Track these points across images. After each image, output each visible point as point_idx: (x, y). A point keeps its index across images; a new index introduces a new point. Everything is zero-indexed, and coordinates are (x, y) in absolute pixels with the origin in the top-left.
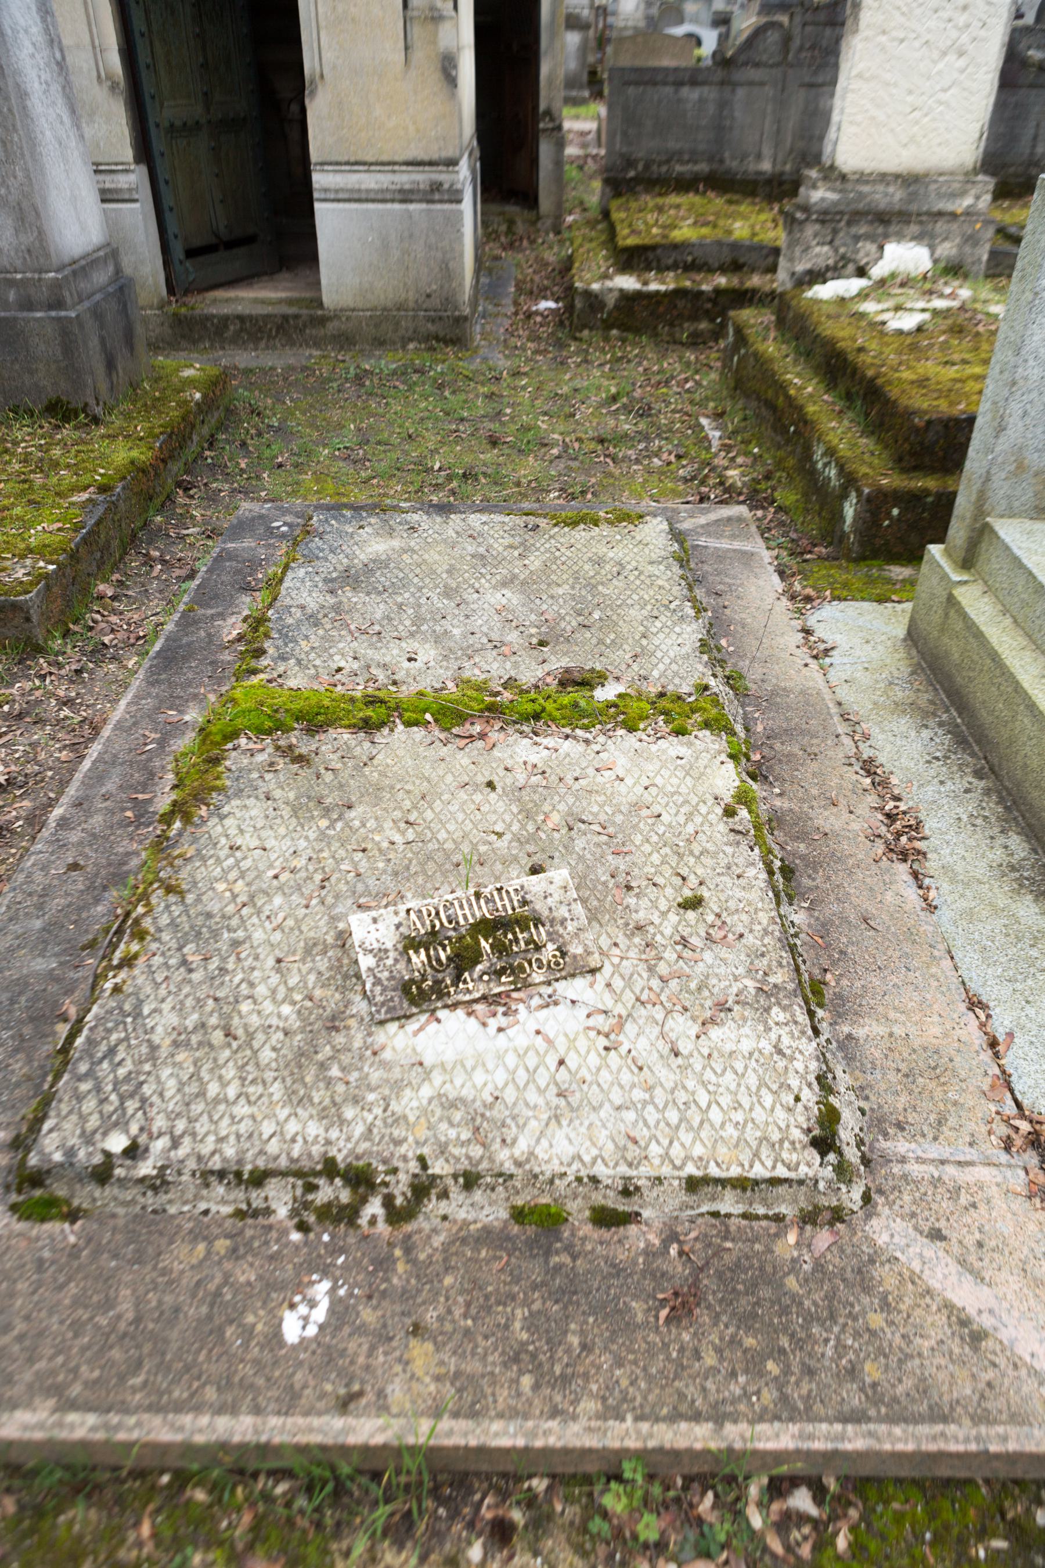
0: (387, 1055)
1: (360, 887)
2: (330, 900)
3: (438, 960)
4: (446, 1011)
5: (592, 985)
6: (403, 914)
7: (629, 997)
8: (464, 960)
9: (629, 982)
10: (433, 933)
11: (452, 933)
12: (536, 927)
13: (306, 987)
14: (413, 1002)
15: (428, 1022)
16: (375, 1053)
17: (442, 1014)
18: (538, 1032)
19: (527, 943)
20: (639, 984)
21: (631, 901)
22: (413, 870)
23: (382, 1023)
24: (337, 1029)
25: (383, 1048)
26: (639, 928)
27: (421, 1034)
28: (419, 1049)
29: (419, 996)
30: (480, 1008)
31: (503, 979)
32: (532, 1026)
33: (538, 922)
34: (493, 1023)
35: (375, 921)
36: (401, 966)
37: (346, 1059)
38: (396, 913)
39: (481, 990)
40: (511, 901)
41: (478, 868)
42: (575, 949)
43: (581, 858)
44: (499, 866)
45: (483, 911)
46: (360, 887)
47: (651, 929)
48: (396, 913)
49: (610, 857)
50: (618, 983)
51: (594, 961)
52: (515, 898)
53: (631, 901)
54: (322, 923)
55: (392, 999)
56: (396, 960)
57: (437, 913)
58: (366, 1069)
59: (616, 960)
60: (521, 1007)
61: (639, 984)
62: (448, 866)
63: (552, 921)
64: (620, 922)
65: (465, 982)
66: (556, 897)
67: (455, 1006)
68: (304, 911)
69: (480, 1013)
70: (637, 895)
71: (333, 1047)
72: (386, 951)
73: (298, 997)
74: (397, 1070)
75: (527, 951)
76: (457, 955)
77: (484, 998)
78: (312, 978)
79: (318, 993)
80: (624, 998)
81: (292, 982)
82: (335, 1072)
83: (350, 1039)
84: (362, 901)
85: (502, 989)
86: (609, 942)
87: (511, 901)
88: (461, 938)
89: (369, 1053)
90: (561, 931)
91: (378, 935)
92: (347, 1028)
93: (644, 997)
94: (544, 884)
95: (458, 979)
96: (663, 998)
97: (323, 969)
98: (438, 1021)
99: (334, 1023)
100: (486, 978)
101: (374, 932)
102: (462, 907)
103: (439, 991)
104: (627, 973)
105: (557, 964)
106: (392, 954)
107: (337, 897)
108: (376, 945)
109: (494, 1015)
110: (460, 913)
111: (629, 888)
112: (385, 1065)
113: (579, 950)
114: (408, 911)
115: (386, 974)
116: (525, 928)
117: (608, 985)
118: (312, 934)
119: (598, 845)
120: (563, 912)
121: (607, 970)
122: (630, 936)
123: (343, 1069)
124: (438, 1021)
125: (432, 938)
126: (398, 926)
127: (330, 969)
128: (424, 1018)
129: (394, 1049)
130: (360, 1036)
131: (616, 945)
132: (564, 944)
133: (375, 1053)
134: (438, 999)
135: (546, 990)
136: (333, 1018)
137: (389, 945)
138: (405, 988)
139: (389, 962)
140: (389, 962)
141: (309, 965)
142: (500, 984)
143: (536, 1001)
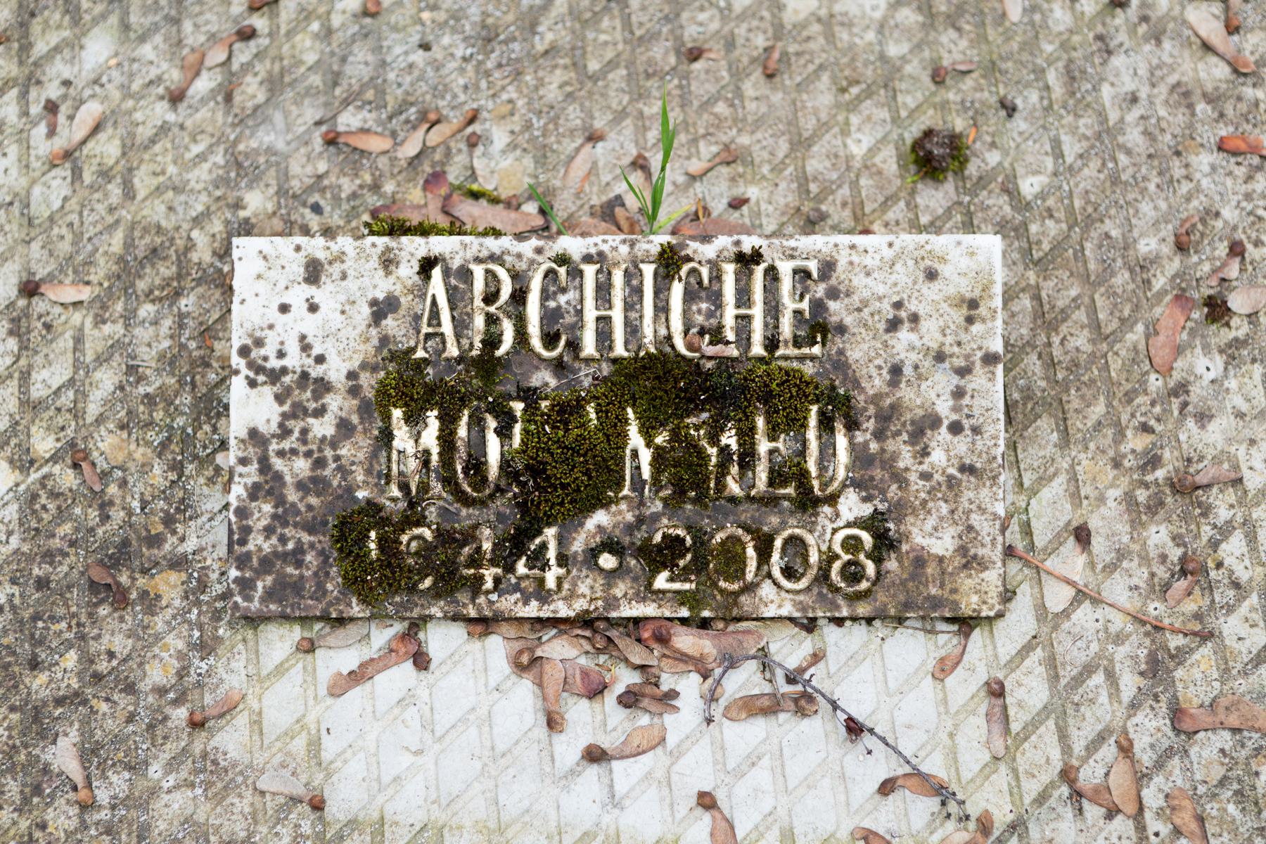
0: (230, 740)
1: (359, 66)
2: (252, 90)
3: (476, 465)
4: (458, 631)
5: (944, 669)
6: (408, 271)
7: (1043, 754)
8: (563, 476)
9: (1067, 690)
10: (487, 363)
11: (544, 378)
12: (826, 424)
13: (76, 412)
14: (356, 584)
15: (389, 656)
16: (196, 724)
17: (442, 639)
18: (706, 801)
19: (777, 478)
20: (1101, 710)
21: (1204, 366)
22: (547, 35)
23: (254, 621)
24: (120, 599)
25: (228, 710)
26: (1186, 488)
27: (356, 693)
28: (330, 747)
29: (379, 565)
30: (561, 651)
31: (661, 581)
32: (697, 771)
33: (839, 409)
34: (588, 721)
35: (314, 272)
36: (355, 451)
37: (109, 715)
38: (388, 262)
39: (584, 594)
40: (773, 309)
41: (752, 86)
42: (932, 536)
43: (1107, 134)
44: (822, 98)
45: (669, 324)
46: (359, 66)
47: (1223, 506)
48: (388, 262)
49: (1203, 160)
50: (1029, 691)
51: (975, 593)
52: (789, 304)
53: (1204, 366)
54: (201, 175)
55: (296, 557)
56: (345, 427)
57: (519, 297)
58: (155, 770)
59: (1058, 597)
60: (689, 687)
61: (1101, 710)
62: (662, 53)
63: (887, 416)
64: (1136, 442)
65: (538, 560)
66: (931, 332)
67: (484, 624)
68: (161, 112)
69: (554, 674)
70: (1232, 352)
71: (88, 660)
72: (323, 386)
73: (44, 444)
74: (243, 804)
75: (769, 501)
76: (536, 470)
77: (586, 621)
78: (106, 380)
79: (107, 445)
80: (1028, 756)
81: (50, 376)
82: (63, 755)
83: (145, 640)
84: (349, 120)
85: (650, 610)
86: (1066, 514)
87: (773, 309)
88: (568, 410)
89: (180, 714)
90: (906, 459)
91: (310, 325)
92: (151, 602)
93: (1090, 775)
94: (904, 275)
95: (517, 543)
96: (1153, 799)
97: (147, 357)
98: (421, 661)
99: (114, 576)
100: (607, 561)
101: (306, 307)
102: (604, 291)
103: (448, 570)
104: (1074, 655)
105: (853, 574)
106: (336, 403)
107: (274, 85)
108: (294, 360)
109: (596, 691)
110: (591, 314)
111: (1217, 310)
112: (214, 775)
113: (943, 544)
114: (427, 266)
115: (302, 466)
116: (791, 423)
117: (996, 691)
118: (156, 212)
119: (1183, 95)
120: (934, 392)
121: (1019, 623)
122: (1140, 513)
123: (89, 753)
124: (421, 661)
125: (480, 382)
126: (382, 309)
127: (169, 361)
128: (382, 636)
129: (257, 723)
130: (176, 643)
131: (1082, 536)
132: (900, 509)
133: (196, 724)
134: (436, 593)
135: (790, 650)
136: (120, 555)
137: (336, 371)
138: (350, 527)
139: (323, 428)
140: (323, 428)
141: (114, 329)
142: (649, 593)
143: (744, 680)
